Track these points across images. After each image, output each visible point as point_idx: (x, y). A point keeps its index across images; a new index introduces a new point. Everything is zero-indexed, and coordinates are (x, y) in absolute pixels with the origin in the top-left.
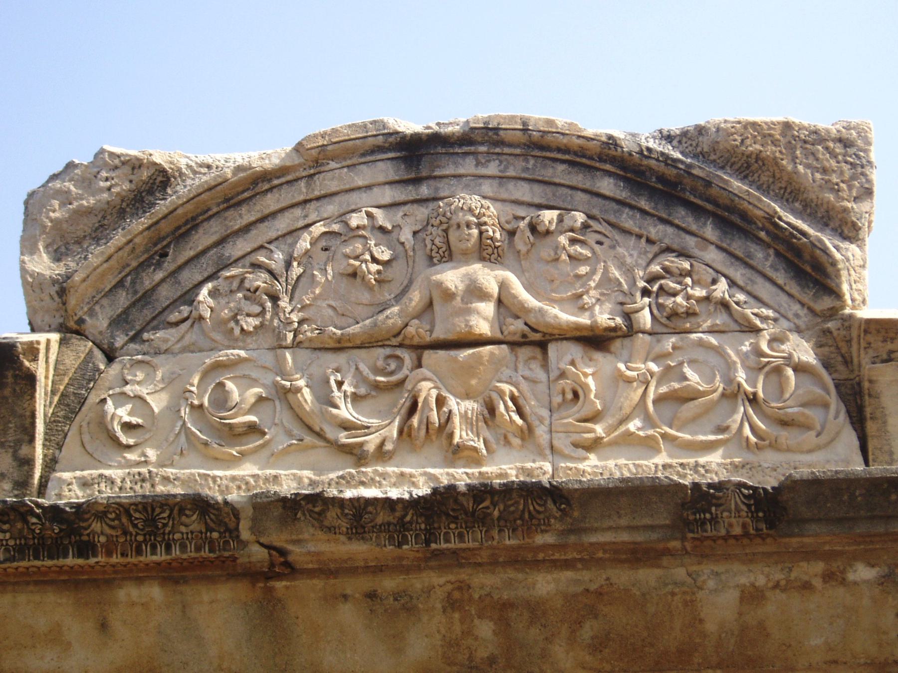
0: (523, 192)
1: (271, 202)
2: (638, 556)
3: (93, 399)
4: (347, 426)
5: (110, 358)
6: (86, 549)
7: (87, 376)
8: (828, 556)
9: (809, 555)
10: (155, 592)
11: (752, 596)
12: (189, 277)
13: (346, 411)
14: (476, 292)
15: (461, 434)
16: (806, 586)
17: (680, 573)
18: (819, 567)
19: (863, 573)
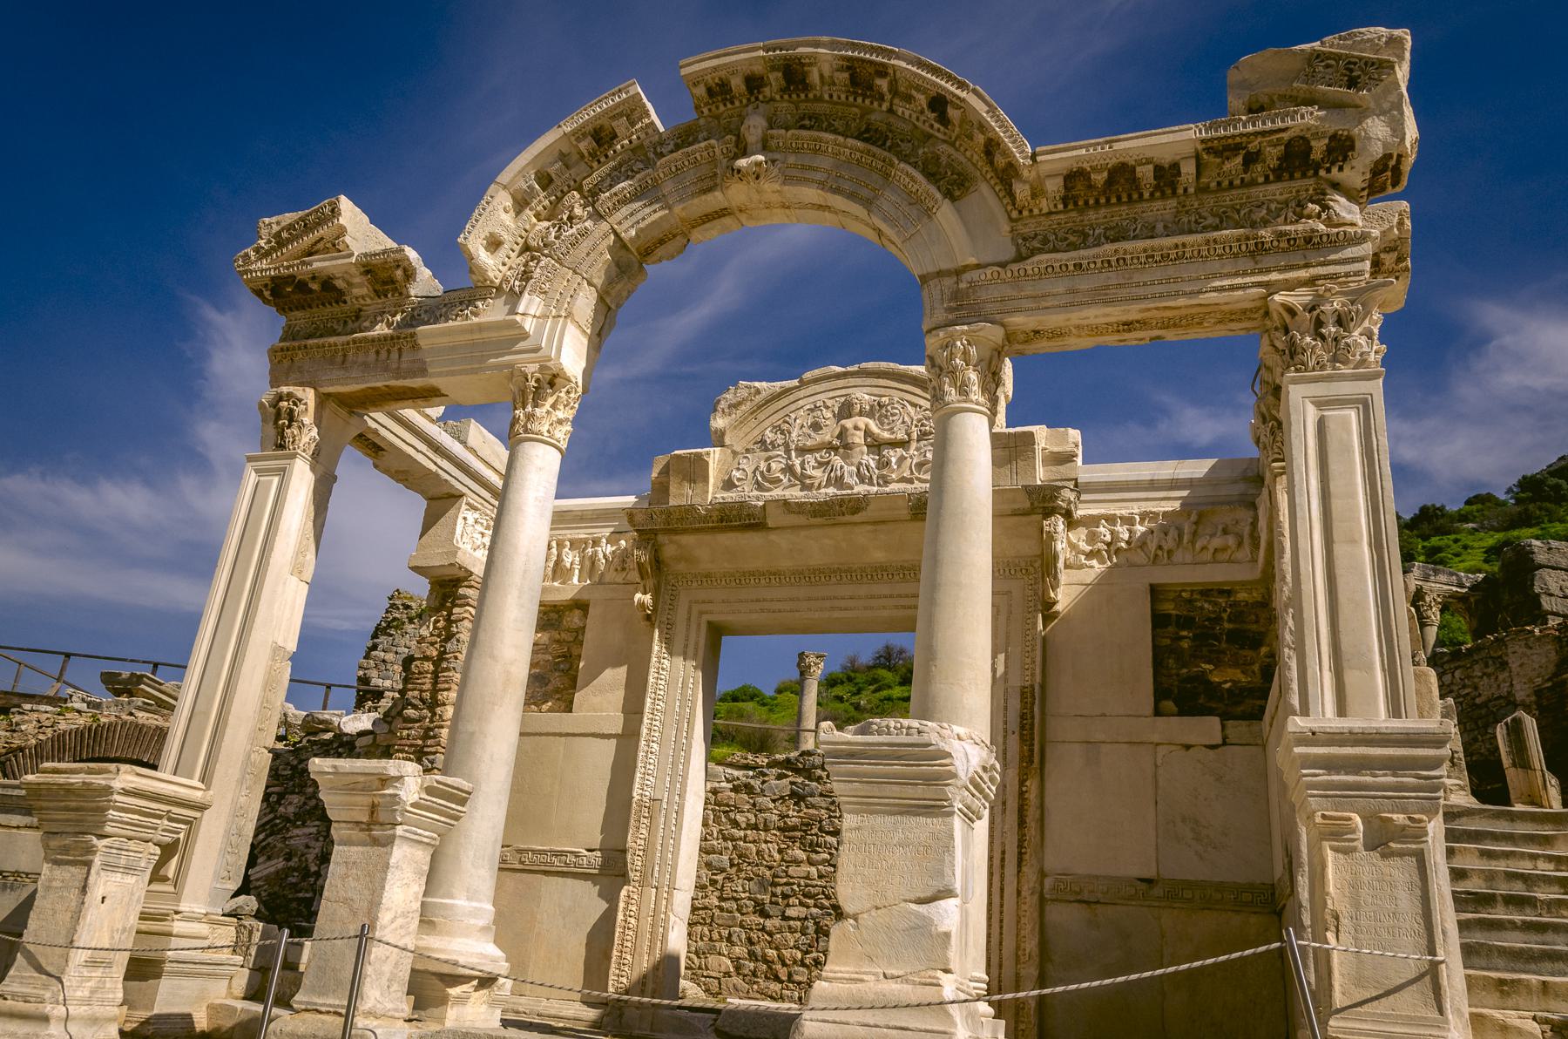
1: (792, 398)
15: (847, 479)
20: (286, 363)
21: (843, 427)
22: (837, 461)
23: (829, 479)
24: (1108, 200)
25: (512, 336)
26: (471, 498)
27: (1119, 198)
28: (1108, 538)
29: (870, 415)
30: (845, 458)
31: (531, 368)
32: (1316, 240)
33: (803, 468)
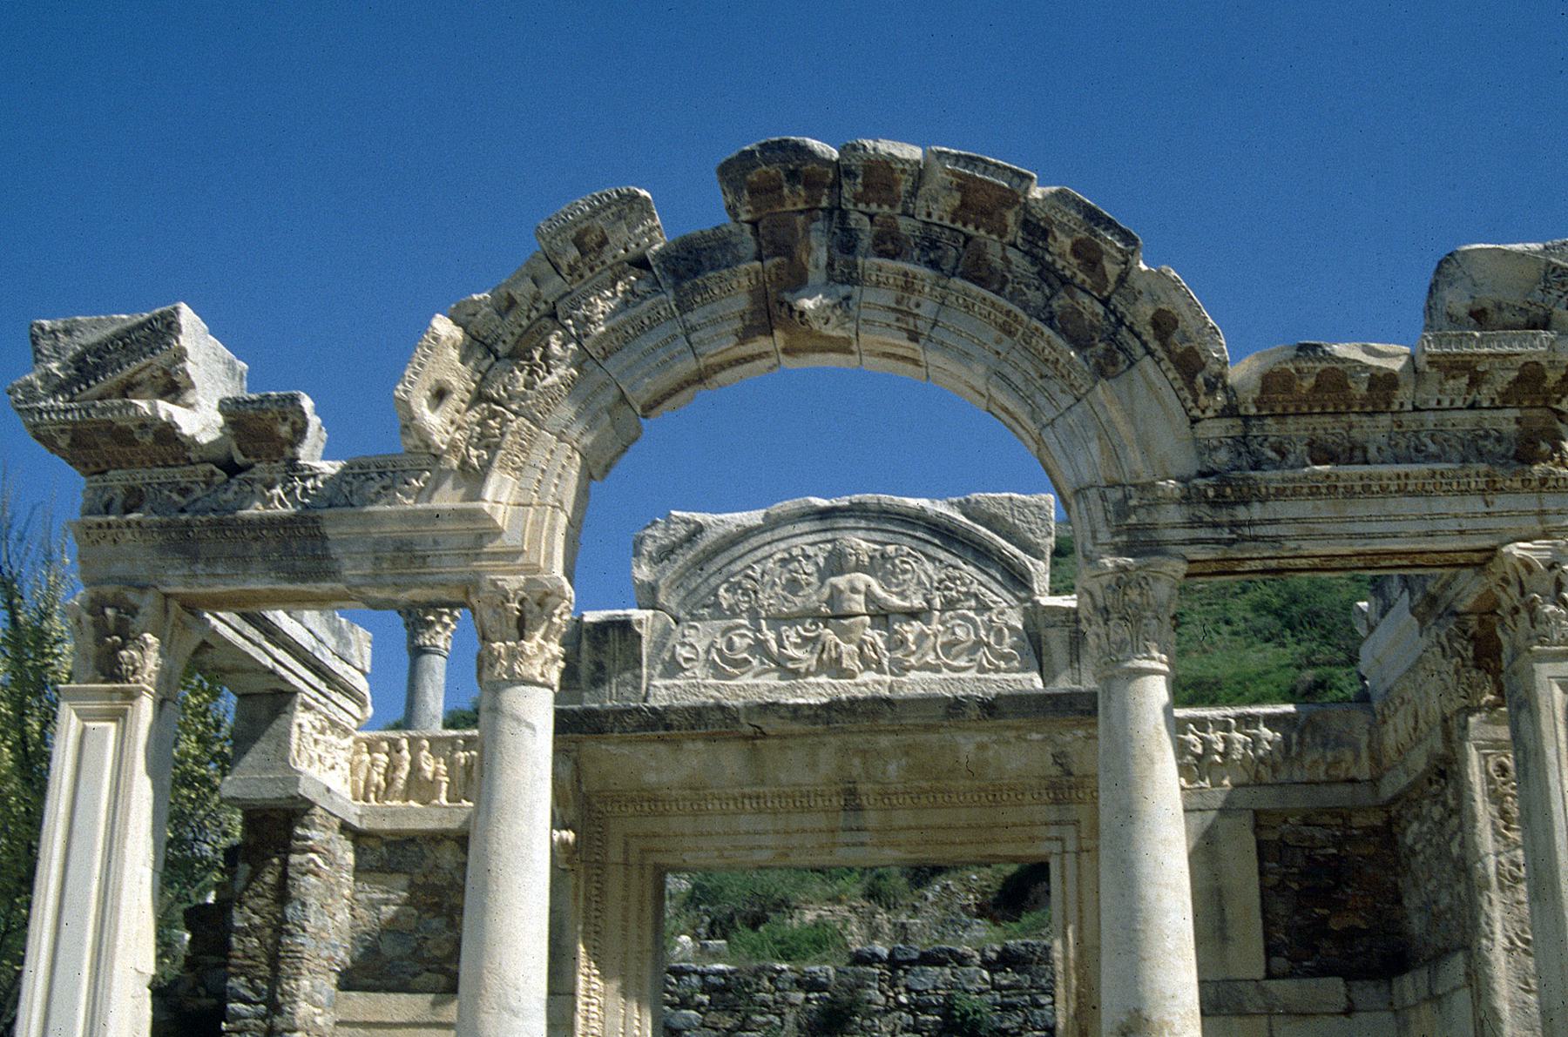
0: (878, 536)
1: (754, 542)
2: (927, 728)
3: (670, 644)
4: (792, 659)
5: (677, 623)
6: (668, 727)
7: (667, 632)
8: (1018, 729)
9: (1008, 727)
10: (700, 745)
11: (982, 747)
12: (713, 581)
13: (791, 651)
14: (854, 590)
15: (846, 663)
16: (1008, 742)
17: (948, 736)
18: (1014, 733)
19: (1035, 736)
20: (106, 546)
21: (834, 587)
22: (829, 635)
23: (820, 659)
24: (1310, 407)
25: (480, 531)
26: (307, 695)
27: (1323, 407)
28: (1199, 750)
29: (869, 570)
30: (843, 633)
31: (513, 583)
32: (1551, 483)
33: (781, 645)
